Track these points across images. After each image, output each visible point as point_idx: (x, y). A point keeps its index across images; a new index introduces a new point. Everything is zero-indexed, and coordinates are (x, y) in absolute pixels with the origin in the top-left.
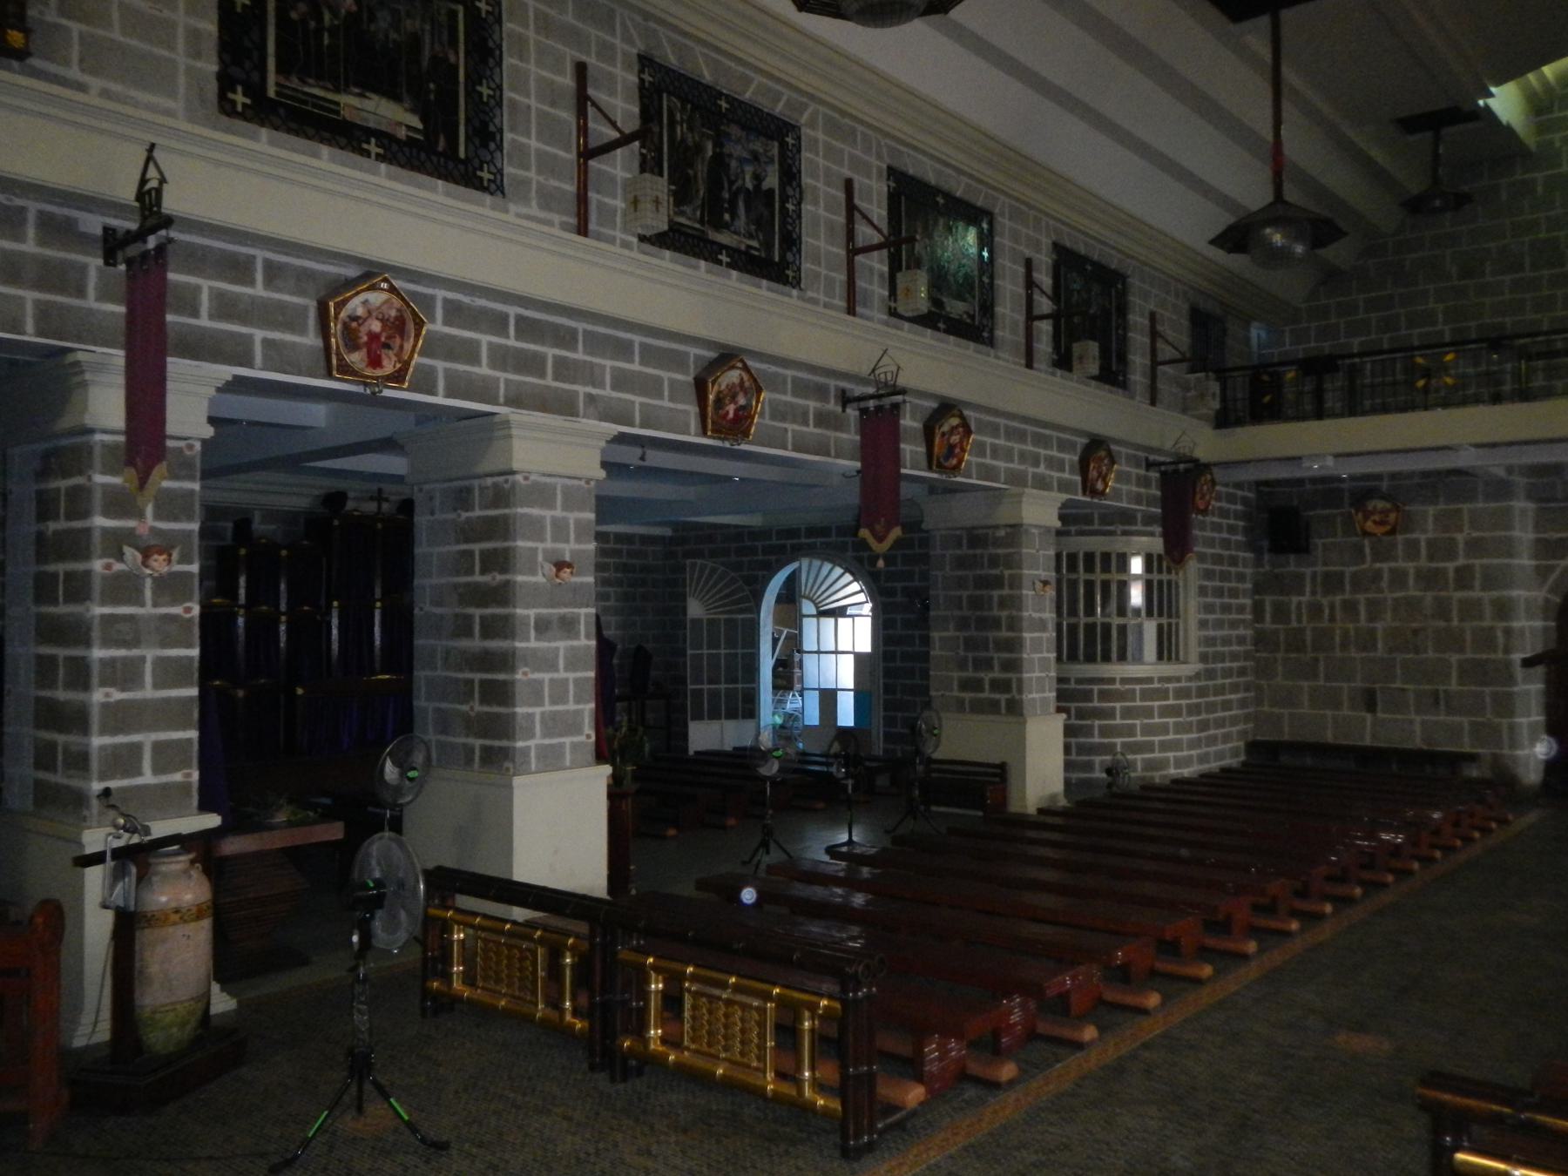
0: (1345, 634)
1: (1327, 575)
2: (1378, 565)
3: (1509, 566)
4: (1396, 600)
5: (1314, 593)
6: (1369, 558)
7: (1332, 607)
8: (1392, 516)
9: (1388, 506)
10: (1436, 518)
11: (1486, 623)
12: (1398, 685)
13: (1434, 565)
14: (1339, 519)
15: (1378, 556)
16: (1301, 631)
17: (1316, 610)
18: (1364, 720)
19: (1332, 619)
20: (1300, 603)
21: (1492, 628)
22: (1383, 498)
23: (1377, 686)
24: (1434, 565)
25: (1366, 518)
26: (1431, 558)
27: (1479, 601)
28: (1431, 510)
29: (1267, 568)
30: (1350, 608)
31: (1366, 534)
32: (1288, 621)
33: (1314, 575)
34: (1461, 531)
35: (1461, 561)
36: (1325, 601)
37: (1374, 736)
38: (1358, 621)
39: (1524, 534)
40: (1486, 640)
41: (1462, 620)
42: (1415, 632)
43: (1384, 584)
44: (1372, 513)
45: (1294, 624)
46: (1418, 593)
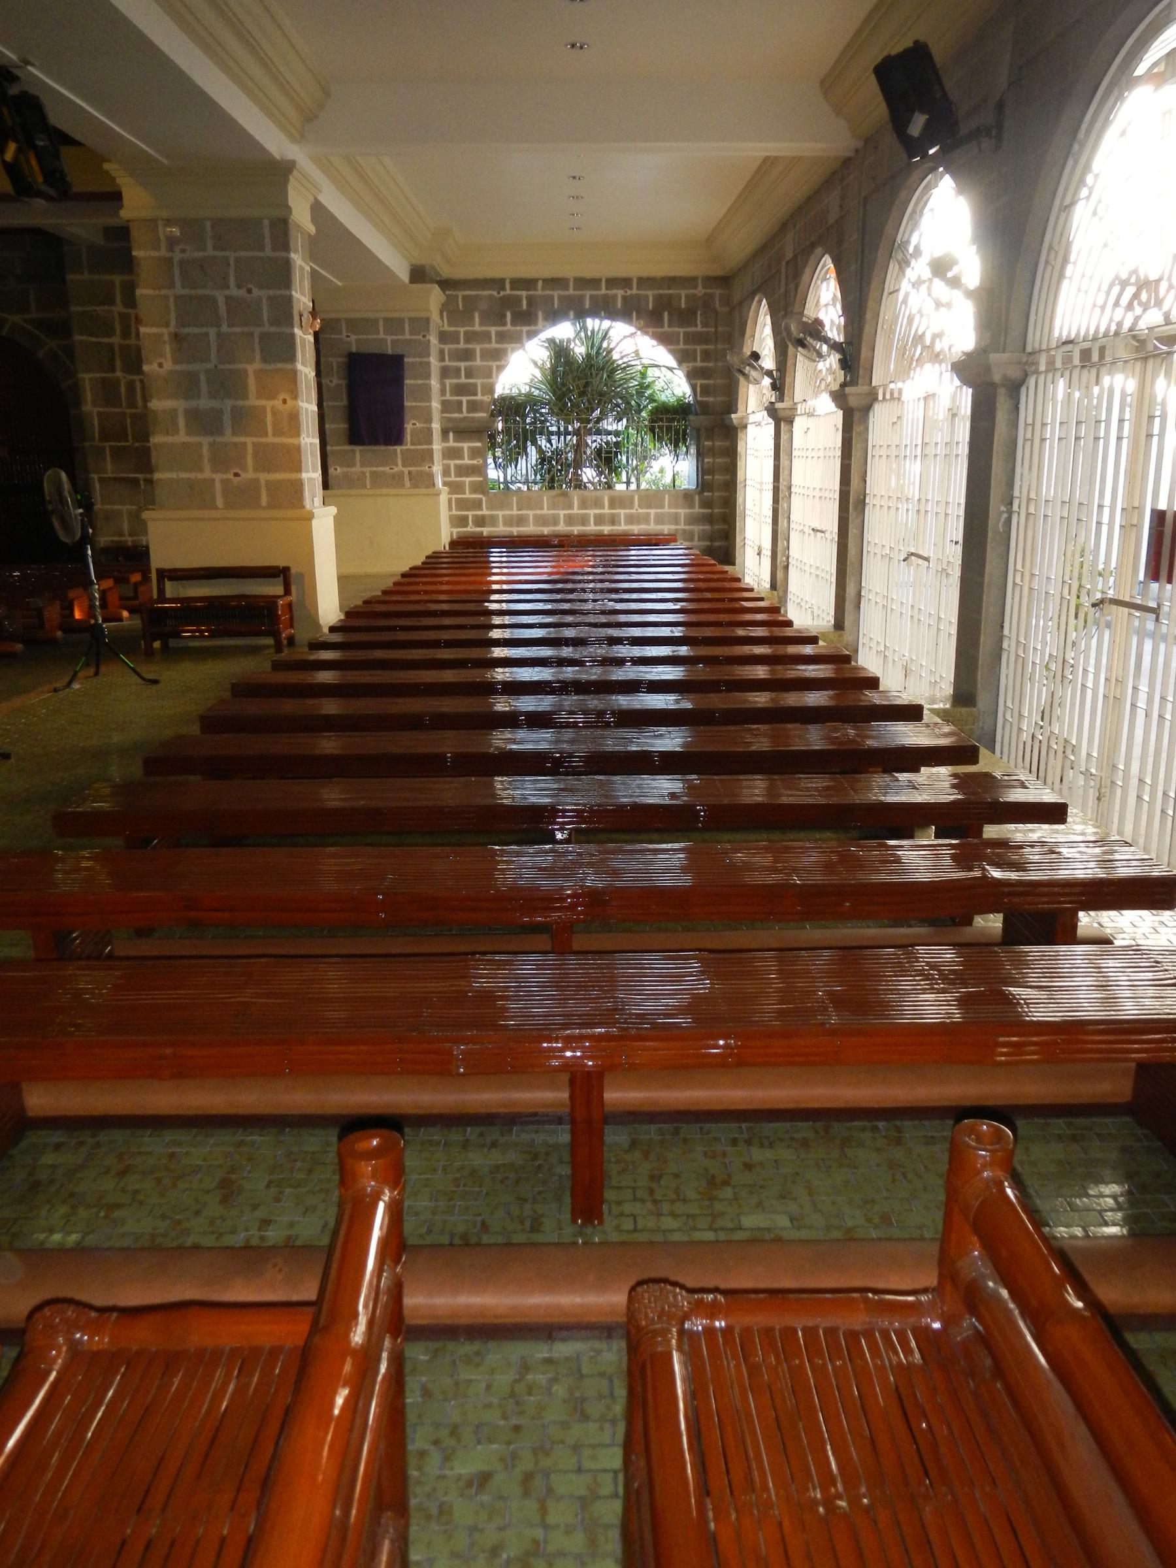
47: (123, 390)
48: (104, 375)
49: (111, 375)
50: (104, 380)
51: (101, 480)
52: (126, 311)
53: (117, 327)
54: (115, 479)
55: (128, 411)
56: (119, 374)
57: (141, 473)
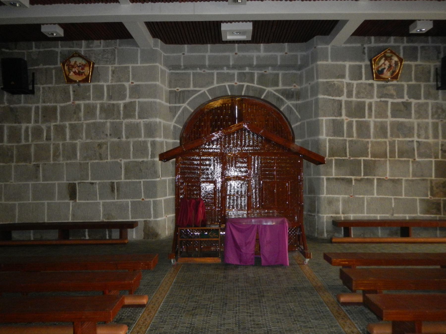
0: (57, 148)
1: (45, 109)
2: (77, 102)
3: (155, 103)
4: (88, 125)
5: (36, 121)
6: (72, 99)
7: (49, 129)
8: (87, 70)
9: (84, 62)
10: (113, 72)
11: (142, 139)
12: (89, 181)
13: (112, 102)
14: (54, 71)
15: (77, 96)
16: (29, 146)
17: (37, 132)
18: (68, 204)
19: (48, 138)
20: (27, 128)
21: (145, 142)
22: (80, 56)
23: (76, 182)
24: (112, 102)
25: (69, 70)
26: (110, 97)
27: (138, 125)
28: (110, 67)
29: (6, 104)
30: (60, 130)
31: (70, 81)
32: (19, 141)
33: (37, 108)
34: (128, 81)
35: (128, 100)
36: (44, 127)
37: (73, 215)
38: (65, 139)
39: (163, 85)
40: (141, 149)
41: (127, 137)
42: (100, 146)
43: (82, 114)
44: (73, 67)
45: (23, 142)
46: (102, 121)
47: (345, 126)
48: (334, 118)
49: (338, 118)
50: (333, 120)
51: (328, 179)
52: (351, 82)
53: (345, 90)
54: (337, 179)
55: (348, 139)
56: (344, 117)
57: (353, 175)
